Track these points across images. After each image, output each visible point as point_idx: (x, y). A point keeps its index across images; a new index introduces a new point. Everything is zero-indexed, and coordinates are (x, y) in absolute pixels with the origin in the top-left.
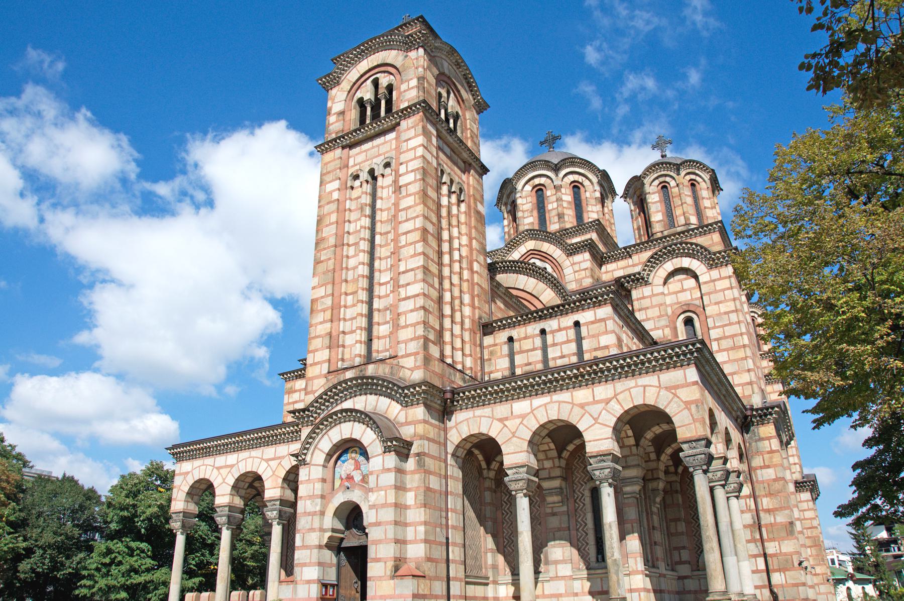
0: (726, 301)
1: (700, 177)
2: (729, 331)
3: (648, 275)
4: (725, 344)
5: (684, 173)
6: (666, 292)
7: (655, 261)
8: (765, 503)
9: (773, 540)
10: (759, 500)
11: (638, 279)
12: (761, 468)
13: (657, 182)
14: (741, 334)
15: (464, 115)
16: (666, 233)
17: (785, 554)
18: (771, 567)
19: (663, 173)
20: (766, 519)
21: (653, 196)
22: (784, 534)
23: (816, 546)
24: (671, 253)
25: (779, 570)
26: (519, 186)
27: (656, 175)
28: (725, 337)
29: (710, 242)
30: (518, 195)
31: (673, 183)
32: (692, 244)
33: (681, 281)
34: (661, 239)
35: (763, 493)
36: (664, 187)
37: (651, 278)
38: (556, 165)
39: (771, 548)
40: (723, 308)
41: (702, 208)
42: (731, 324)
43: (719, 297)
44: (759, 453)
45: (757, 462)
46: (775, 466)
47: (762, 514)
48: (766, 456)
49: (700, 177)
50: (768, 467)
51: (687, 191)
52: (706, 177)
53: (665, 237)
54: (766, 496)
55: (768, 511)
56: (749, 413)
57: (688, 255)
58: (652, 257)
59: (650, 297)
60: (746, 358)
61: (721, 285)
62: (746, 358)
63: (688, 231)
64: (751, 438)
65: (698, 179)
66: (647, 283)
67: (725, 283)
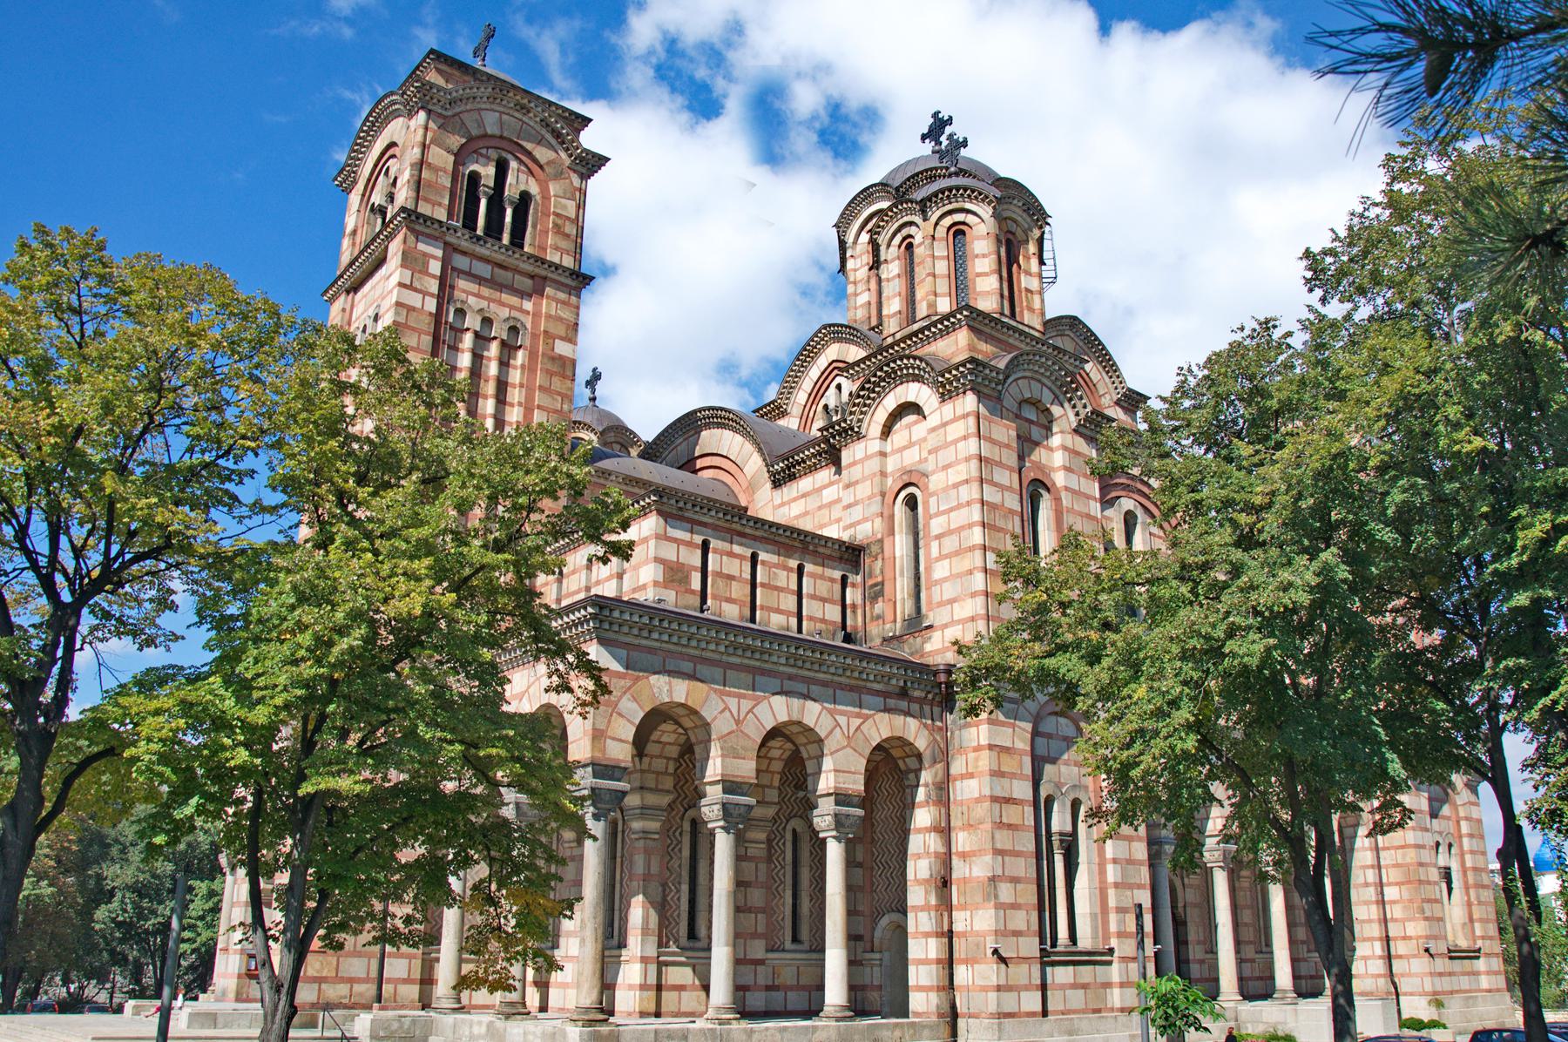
0: (957, 462)
1: (975, 214)
2: (958, 519)
3: (860, 421)
4: (950, 544)
5: (939, 213)
6: (889, 450)
7: (869, 393)
8: (961, 840)
9: (963, 907)
10: (953, 835)
11: (845, 430)
12: (962, 777)
13: (898, 238)
14: (970, 526)
15: (546, 196)
16: (898, 336)
17: (978, 934)
18: (956, 955)
19: (906, 219)
20: (959, 869)
21: (891, 266)
22: (979, 898)
23: (1409, 882)
24: (895, 379)
25: (966, 961)
26: (850, 239)
27: (896, 225)
28: (949, 532)
29: (953, 349)
30: (849, 254)
31: (916, 241)
32: (915, 358)
33: (909, 426)
34: (891, 346)
35: (959, 823)
36: (910, 247)
37: (865, 425)
38: (897, 189)
39: (961, 921)
40: (955, 475)
41: (970, 276)
42: (959, 506)
43: (947, 456)
44: (962, 749)
45: (957, 767)
46: (981, 774)
47: (955, 861)
48: (972, 755)
49: (975, 214)
50: (971, 776)
51: (941, 250)
52: (985, 211)
53: (897, 343)
54: (963, 829)
55: (964, 856)
56: (942, 678)
57: (917, 379)
58: (863, 388)
59: (862, 461)
60: (970, 572)
61: (957, 430)
62: (970, 572)
63: (928, 328)
64: (954, 722)
65: (970, 219)
66: (859, 436)
67: (957, 430)
